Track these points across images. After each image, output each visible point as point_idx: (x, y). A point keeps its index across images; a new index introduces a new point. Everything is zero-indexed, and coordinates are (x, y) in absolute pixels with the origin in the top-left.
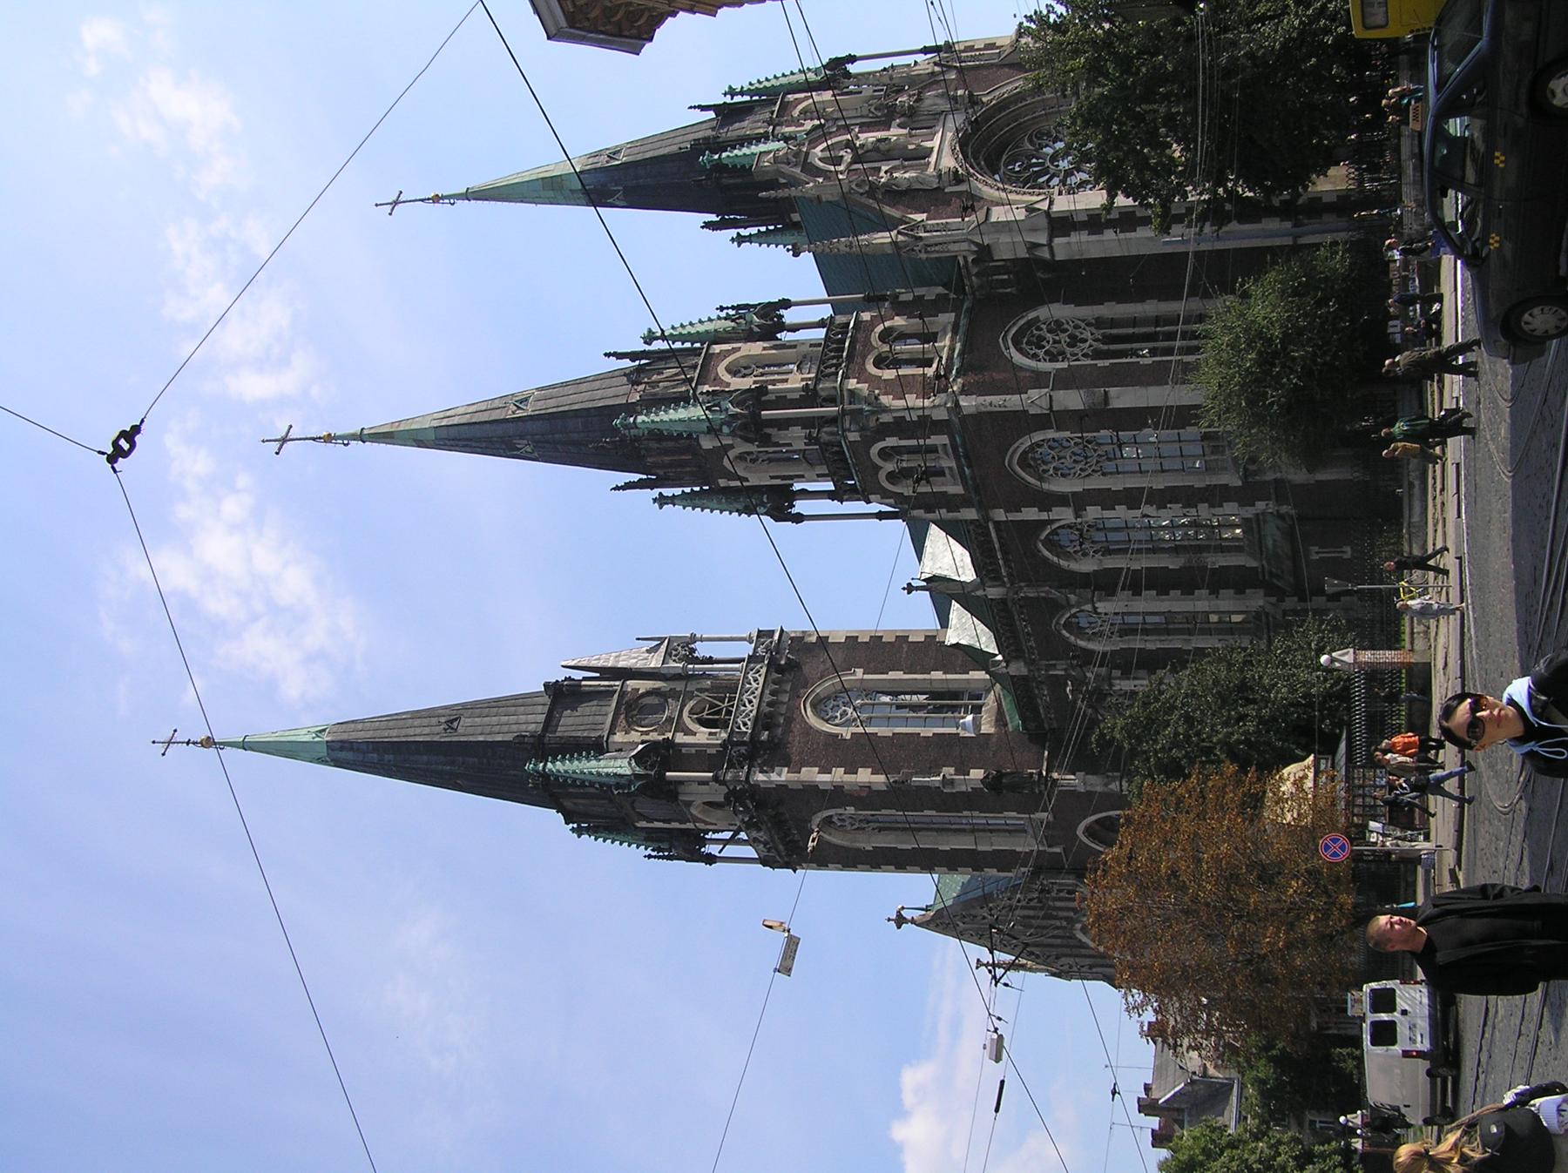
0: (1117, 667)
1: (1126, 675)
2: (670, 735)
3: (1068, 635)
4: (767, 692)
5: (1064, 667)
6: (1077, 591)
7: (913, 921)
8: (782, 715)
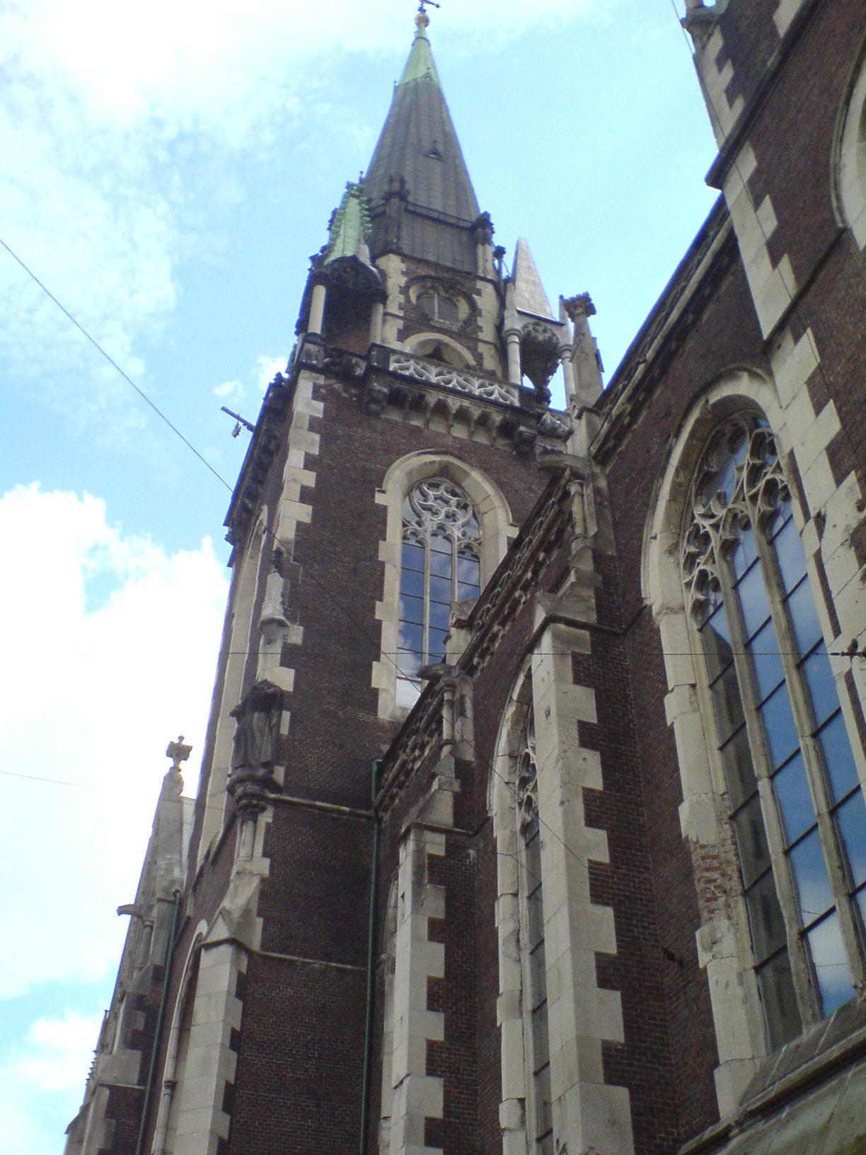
0: (454, 849)
1: (430, 870)
2: (393, 307)
3: (515, 697)
4: (466, 403)
5: (458, 737)
6: (590, 593)
7: (175, 769)
8: (427, 424)
